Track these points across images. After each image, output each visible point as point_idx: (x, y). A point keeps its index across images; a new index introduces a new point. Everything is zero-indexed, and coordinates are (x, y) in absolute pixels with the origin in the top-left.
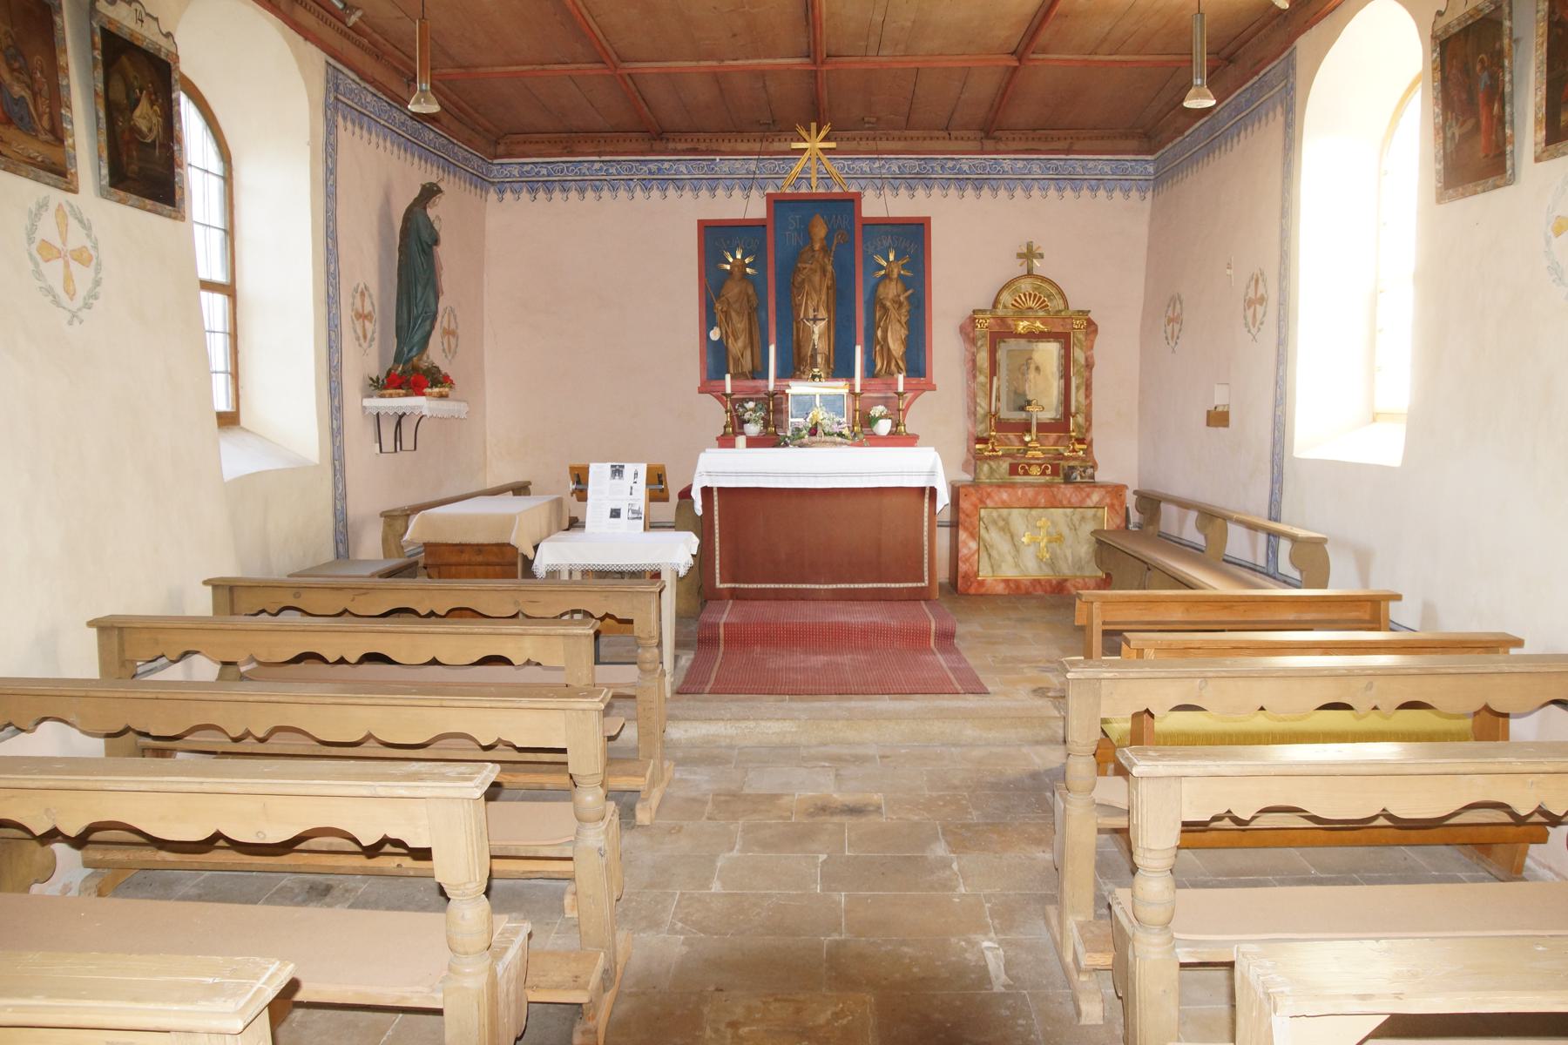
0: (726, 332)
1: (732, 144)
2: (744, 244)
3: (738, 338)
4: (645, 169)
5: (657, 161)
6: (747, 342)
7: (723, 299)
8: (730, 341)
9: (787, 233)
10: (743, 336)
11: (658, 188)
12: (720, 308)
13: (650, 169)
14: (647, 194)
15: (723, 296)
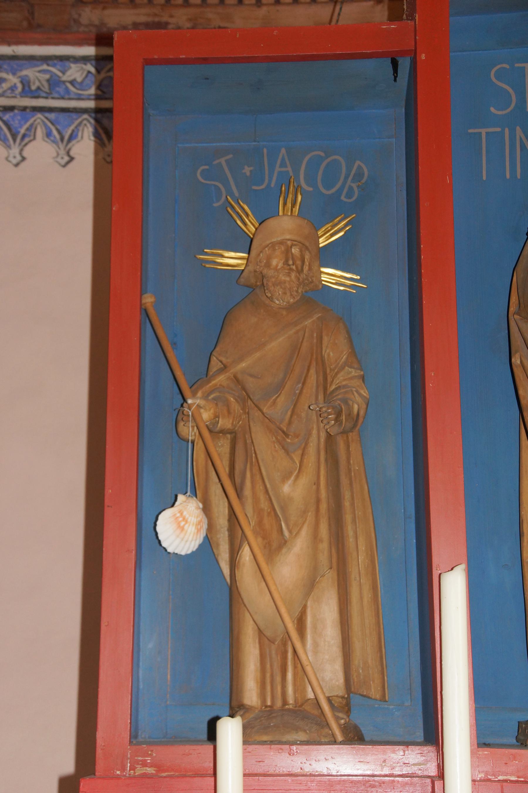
0: (232, 515)
1: (264, 10)
2: (311, 179)
3: (283, 543)
4: (13, 80)
5: (46, 59)
6: (323, 558)
7: (221, 379)
8: (246, 553)
9: (483, 131)
10: (305, 533)
11: (49, 134)
12: (206, 415)
13: (25, 83)
14: (15, 150)
15: (225, 368)
